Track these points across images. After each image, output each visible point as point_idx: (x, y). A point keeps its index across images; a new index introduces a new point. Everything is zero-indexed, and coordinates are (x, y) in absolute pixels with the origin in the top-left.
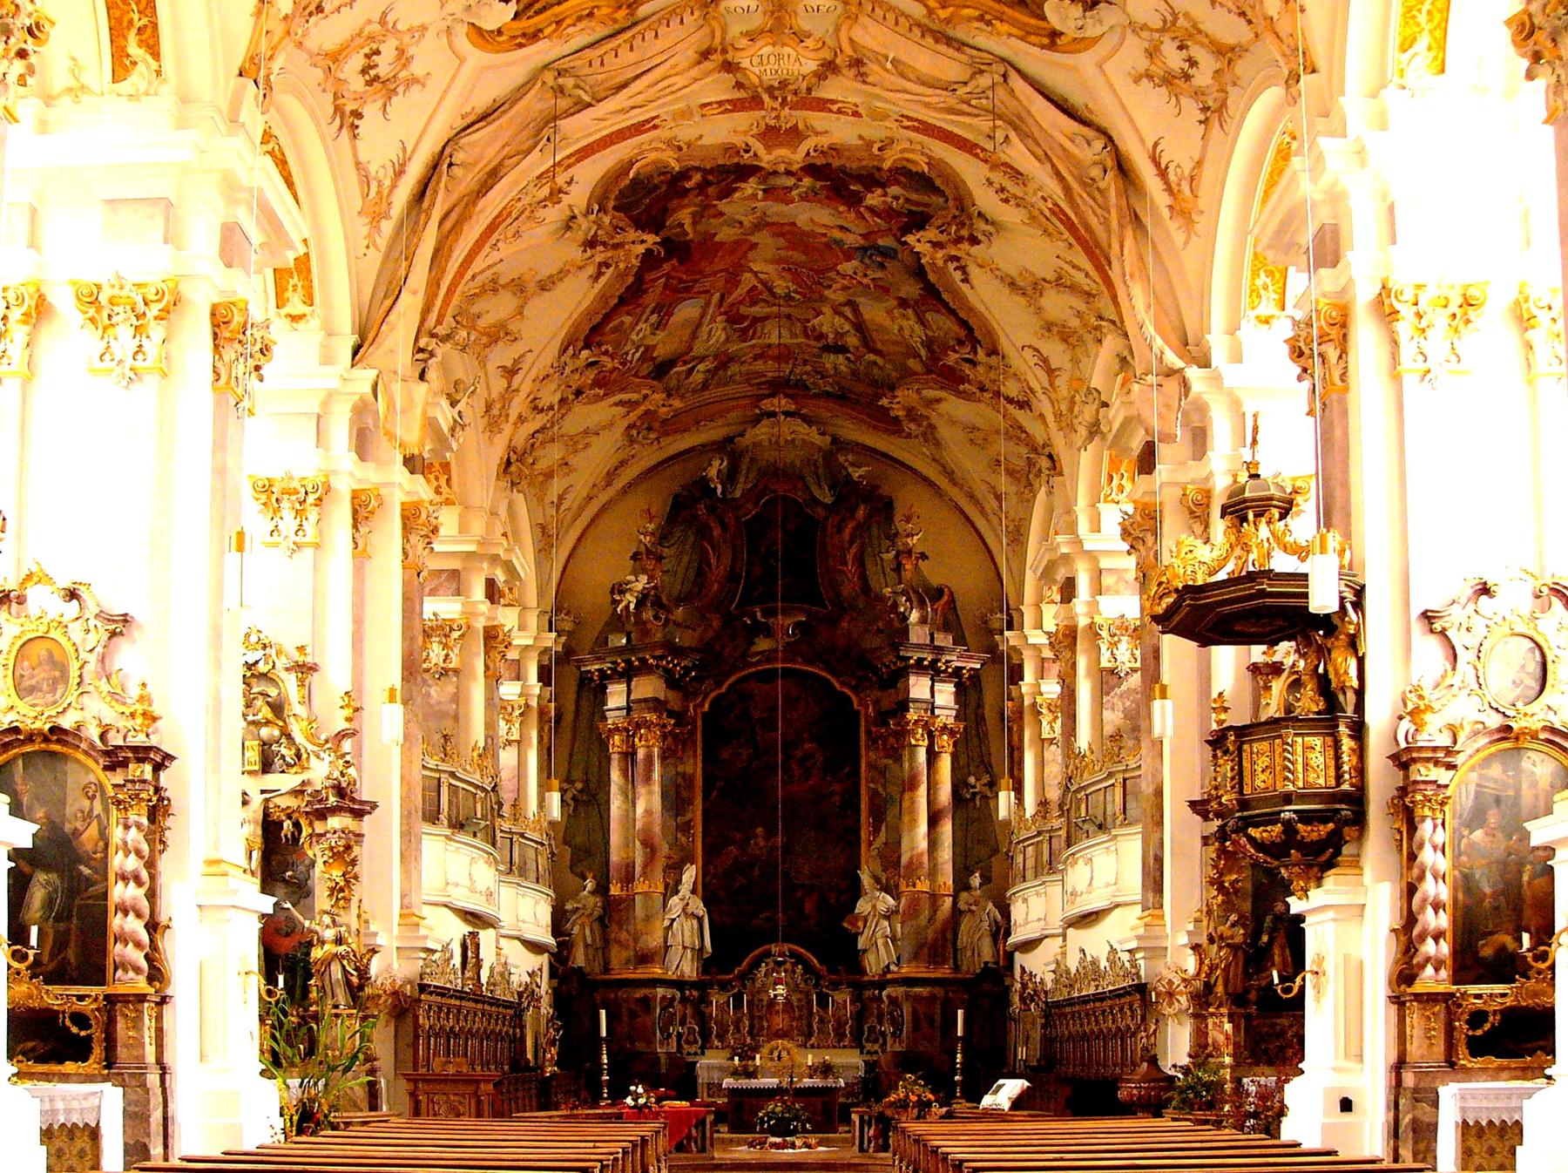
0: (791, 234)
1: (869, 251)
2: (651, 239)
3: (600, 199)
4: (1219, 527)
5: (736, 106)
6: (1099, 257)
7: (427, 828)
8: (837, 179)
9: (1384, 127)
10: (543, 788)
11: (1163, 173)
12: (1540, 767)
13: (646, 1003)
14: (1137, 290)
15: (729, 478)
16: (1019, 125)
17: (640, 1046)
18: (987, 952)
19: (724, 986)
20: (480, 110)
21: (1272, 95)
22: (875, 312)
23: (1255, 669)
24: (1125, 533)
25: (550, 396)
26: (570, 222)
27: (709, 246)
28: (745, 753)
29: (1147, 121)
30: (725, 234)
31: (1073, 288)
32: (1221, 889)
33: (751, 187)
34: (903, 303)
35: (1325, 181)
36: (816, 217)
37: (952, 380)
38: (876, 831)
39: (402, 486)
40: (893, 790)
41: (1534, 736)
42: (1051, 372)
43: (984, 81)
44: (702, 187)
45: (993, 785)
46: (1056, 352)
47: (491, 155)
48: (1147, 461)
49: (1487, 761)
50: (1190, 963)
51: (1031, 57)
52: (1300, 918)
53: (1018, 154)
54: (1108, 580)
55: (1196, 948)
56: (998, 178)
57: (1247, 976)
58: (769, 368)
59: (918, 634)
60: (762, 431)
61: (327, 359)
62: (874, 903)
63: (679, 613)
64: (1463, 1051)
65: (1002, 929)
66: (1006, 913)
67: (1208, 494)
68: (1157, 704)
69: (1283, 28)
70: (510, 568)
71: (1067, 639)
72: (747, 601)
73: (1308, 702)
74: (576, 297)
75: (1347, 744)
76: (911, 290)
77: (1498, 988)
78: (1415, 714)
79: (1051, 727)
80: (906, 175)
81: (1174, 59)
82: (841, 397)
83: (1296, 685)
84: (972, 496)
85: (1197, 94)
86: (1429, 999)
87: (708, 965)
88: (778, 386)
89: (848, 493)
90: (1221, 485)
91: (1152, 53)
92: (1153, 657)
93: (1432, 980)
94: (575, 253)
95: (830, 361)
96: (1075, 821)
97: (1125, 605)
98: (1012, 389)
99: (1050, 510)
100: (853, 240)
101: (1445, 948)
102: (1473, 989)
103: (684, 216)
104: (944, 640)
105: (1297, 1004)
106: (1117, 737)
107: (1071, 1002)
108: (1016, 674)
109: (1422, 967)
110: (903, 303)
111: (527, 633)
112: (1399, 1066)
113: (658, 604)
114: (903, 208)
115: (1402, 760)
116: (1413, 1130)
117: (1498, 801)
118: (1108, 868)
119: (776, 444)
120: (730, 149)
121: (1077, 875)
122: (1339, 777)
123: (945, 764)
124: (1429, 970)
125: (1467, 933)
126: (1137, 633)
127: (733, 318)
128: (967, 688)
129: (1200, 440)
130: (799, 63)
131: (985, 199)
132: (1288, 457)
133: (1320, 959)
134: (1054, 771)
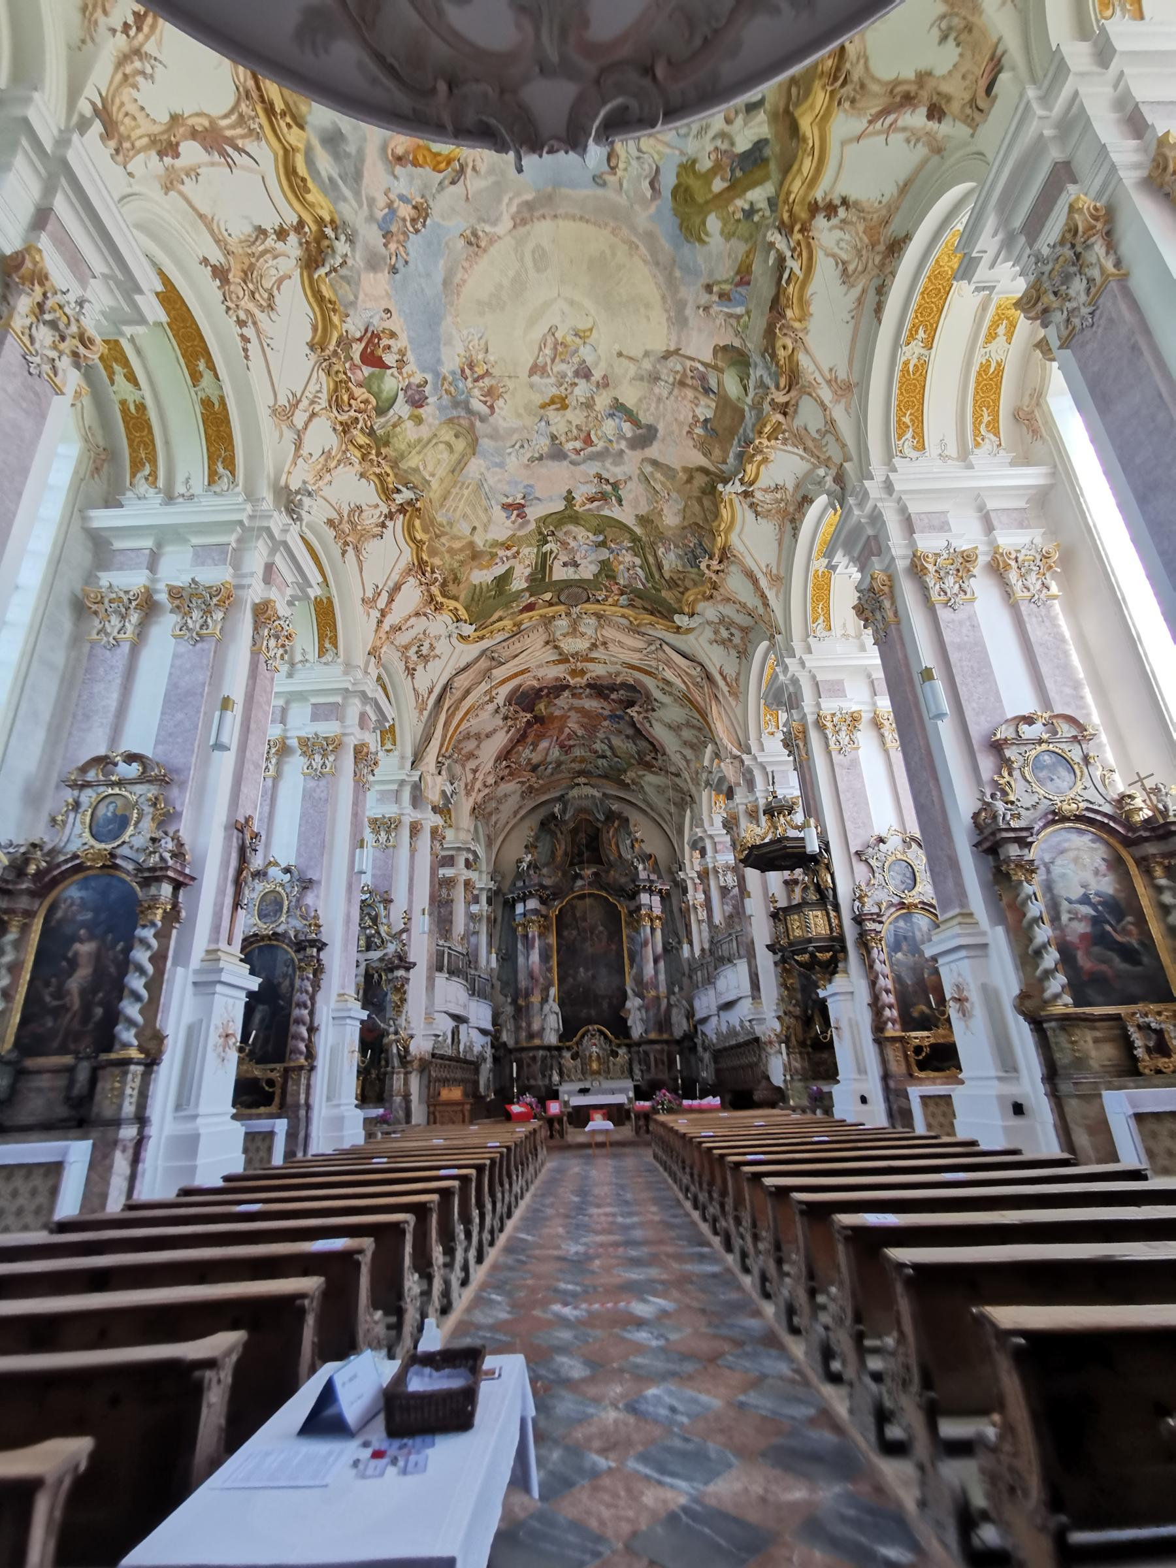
0: (582, 711)
1: (613, 717)
2: (529, 715)
3: (509, 701)
4: (763, 819)
5: (560, 662)
6: (703, 715)
7: (437, 974)
8: (599, 689)
9: (810, 652)
10: (489, 952)
11: (724, 678)
12: (922, 921)
13: (534, 1058)
14: (719, 724)
15: (564, 811)
16: (669, 663)
17: (532, 1082)
18: (685, 1026)
19: (569, 1049)
20: (462, 664)
21: (765, 644)
22: (616, 741)
23: (786, 882)
24: (724, 826)
25: (491, 780)
26: (497, 711)
27: (552, 718)
28: (575, 933)
29: (716, 658)
30: (557, 713)
31: (693, 727)
32: (787, 988)
33: (566, 693)
34: (627, 737)
35: (789, 674)
36: (592, 704)
37: (648, 766)
38: (632, 967)
39: (432, 820)
40: (638, 948)
41: (916, 906)
42: (687, 761)
43: (653, 648)
44: (547, 695)
45: (680, 942)
46: (688, 753)
47: (466, 684)
48: (730, 795)
49: (896, 919)
50: (777, 1026)
51: (670, 637)
52: (824, 1000)
53: (669, 674)
54: (719, 847)
55: (779, 1018)
56: (661, 684)
57: (805, 1032)
58: (576, 766)
59: (643, 875)
60: (574, 793)
61: (402, 767)
62: (633, 1003)
63: (545, 871)
64: (915, 1068)
65: (690, 1014)
66: (692, 1006)
67: (757, 807)
68: (747, 901)
69: (766, 619)
70: (475, 853)
71: (704, 875)
72: (572, 864)
73: (813, 896)
74: (500, 740)
75: (832, 914)
76: (630, 731)
77: (925, 1034)
78: (860, 898)
79: (702, 914)
80: (624, 685)
81: (725, 634)
82: (606, 777)
83: (805, 889)
84: (660, 815)
85: (735, 647)
86: (893, 1039)
87: (561, 1038)
88: (581, 773)
89: (611, 816)
90: (762, 803)
91: (716, 632)
92: (742, 881)
93: (892, 1031)
94: (501, 723)
95: (600, 762)
96: (717, 958)
97: (728, 858)
98: (673, 769)
99: (692, 818)
100: (606, 713)
101: (895, 1013)
102: (913, 1034)
103: (542, 706)
104: (653, 877)
105: (830, 1046)
106: (731, 916)
107: (725, 1049)
108: (685, 891)
109: (885, 1023)
110: (627, 737)
111: (482, 881)
112: (886, 1077)
113: (536, 867)
114: (623, 697)
115: (859, 920)
116: (899, 1113)
117: (905, 938)
118: (733, 980)
119: (580, 798)
120: (557, 679)
121: (721, 983)
122: (831, 930)
123: (659, 933)
124: (890, 1025)
125: (904, 1004)
126: (735, 869)
127: (562, 746)
128: (665, 897)
129: (751, 784)
130: (581, 645)
131: (657, 694)
132: (789, 788)
133: (837, 1021)
134: (706, 935)
